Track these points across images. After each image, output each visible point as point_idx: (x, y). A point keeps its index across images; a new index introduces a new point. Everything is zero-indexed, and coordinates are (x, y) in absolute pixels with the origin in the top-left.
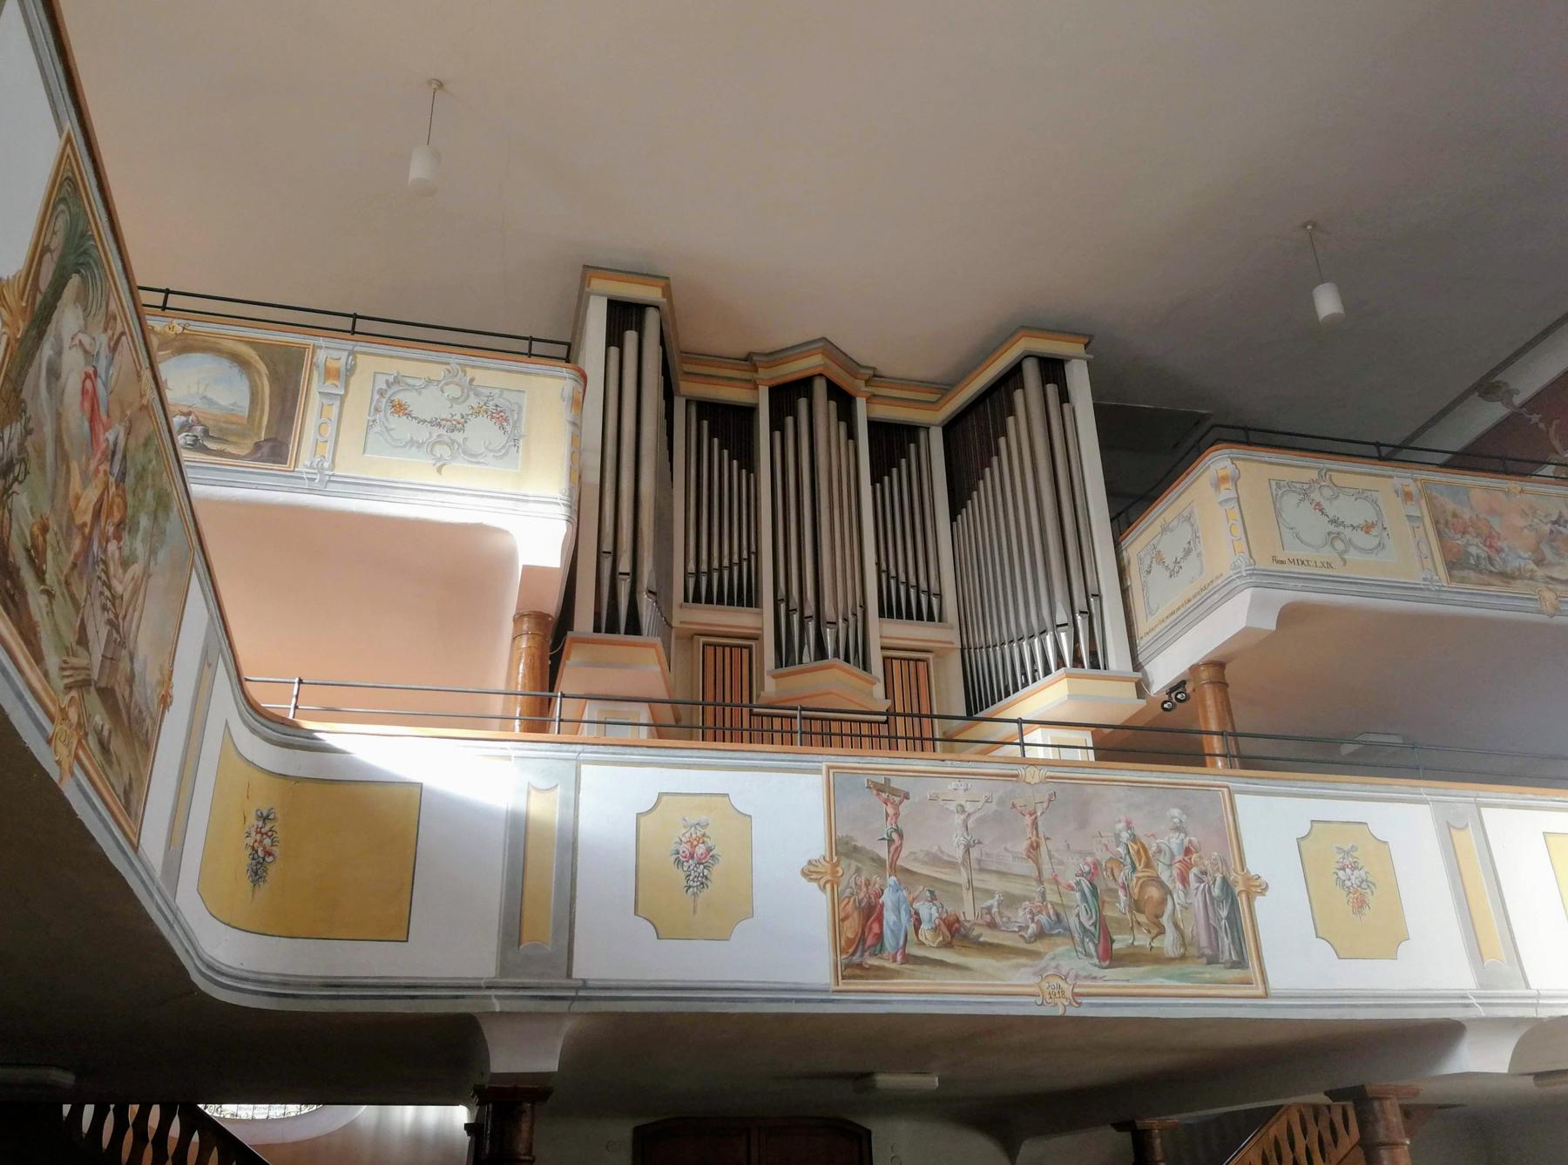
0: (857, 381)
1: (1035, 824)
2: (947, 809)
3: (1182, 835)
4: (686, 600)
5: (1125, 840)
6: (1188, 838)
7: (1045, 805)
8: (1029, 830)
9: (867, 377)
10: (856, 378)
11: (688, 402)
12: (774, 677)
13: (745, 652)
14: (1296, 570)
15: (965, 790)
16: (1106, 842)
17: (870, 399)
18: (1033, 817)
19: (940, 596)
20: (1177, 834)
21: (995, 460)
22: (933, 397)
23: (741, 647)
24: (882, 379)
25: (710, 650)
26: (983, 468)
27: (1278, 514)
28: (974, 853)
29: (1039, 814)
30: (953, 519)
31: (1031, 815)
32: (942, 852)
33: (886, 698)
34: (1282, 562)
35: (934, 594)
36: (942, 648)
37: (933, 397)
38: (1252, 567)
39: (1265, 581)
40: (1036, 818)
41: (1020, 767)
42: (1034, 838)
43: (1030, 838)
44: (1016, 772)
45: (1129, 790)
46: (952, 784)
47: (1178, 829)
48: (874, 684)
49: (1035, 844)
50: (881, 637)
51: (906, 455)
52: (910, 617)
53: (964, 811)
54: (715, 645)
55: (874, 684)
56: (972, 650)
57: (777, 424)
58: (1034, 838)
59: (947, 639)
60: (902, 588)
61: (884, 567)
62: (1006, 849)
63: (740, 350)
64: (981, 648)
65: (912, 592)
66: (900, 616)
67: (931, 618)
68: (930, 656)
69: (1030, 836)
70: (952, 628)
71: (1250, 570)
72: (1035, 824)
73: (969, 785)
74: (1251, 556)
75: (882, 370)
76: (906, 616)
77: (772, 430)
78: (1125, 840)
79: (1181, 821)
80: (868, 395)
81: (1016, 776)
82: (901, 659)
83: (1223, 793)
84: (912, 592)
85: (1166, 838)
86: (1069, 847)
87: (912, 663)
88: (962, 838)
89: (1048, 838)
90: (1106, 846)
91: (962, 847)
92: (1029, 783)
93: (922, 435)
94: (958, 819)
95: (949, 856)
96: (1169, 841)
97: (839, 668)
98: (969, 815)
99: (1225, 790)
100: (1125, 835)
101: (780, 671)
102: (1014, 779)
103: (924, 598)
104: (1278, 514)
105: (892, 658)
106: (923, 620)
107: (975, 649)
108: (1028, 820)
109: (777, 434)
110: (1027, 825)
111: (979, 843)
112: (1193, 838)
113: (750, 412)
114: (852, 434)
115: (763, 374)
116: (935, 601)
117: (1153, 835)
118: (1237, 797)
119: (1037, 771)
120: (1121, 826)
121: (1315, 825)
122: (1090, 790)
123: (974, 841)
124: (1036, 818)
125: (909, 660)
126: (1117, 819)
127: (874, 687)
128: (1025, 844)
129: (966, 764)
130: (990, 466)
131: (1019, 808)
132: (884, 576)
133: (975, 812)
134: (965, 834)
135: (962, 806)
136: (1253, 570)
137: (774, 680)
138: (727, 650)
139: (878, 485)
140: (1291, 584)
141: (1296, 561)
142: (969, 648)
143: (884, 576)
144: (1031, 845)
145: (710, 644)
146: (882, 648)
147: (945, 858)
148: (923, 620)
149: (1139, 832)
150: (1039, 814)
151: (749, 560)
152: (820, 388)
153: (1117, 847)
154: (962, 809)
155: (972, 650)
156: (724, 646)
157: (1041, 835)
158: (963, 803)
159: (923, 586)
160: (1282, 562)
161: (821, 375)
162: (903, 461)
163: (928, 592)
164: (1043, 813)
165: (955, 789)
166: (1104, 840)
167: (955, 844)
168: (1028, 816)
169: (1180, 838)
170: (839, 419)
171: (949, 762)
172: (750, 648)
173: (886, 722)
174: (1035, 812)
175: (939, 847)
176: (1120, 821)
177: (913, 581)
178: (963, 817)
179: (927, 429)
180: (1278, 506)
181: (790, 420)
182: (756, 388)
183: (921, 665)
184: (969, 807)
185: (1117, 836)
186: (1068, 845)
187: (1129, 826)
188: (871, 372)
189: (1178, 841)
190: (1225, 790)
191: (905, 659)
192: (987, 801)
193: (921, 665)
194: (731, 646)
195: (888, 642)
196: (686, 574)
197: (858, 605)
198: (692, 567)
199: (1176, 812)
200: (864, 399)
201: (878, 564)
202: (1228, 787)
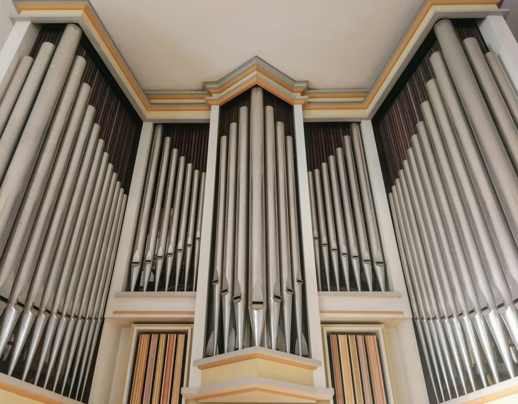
0: (294, 94)
4: (128, 288)
9: (302, 90)
10: (293, 92)
11: (155, 125)
12: (202, 367)
13: (181, 337)
17: (305, 107)
19: (384, 263)
21: (420, 126)
22: (361, 99)
23: (177, 333)
24: (316, 91)
25: (145, 338)
26: (410, 137)
30: (389, 190)
35: (378, 263)
36: (394, 319)
37: (361, 99)
48: (316, 368)
50: (321, 312)
51: (341, 145)
52: (354, 287)
54: (150, 333)
55: (313, 368)
56: (425, 320)
57: (223, 130)
61: (324, 240)
63: (195, 83)
64: (434, 318)
65: (355, 263)
66: (343, 287)
67: (376, 287)
75: (315, 83)
76: (350, 287)
77: (220, 135)
80: (303, 102)
82: (348, 334)
84: (355, 263)
87: (360, 338)
93: (355, 130)
97: (263, 357)
101: (208, 360)
103: (367, 267)
105: (337, 333)
106: (380, 290)
107: (428, 319)
109: (224, 138)
113: (205, 127)
114: (290, 131)
115: (215, 96)
125: (356, 334)
127: (314, 371)
130: (417, 132)
132: (325, 249)
137: (201, 371)
139: (317, 171)
142: (422, 319)
143: (325, 249)
145: (146, 333)
146: (323, 323)
148: (380, 290)
152: (257, 98)
155: (425, 320)
156: (159, 333)
159: (366, 255)
161: (256, 86)
162: (339, 150)
170: (276, 119)
172: (185, 333)
177: (354, 252)
179: (359, 123)
181: (233, 126)
182: (210, 109)
183: (371, 339)
188: (305, 85)
194: (167, 333)
195: (329, 317)
196: (131, 264)
197: (295, 280)
198: (137, 257)
200: (301, 106)
201: (319, 238)
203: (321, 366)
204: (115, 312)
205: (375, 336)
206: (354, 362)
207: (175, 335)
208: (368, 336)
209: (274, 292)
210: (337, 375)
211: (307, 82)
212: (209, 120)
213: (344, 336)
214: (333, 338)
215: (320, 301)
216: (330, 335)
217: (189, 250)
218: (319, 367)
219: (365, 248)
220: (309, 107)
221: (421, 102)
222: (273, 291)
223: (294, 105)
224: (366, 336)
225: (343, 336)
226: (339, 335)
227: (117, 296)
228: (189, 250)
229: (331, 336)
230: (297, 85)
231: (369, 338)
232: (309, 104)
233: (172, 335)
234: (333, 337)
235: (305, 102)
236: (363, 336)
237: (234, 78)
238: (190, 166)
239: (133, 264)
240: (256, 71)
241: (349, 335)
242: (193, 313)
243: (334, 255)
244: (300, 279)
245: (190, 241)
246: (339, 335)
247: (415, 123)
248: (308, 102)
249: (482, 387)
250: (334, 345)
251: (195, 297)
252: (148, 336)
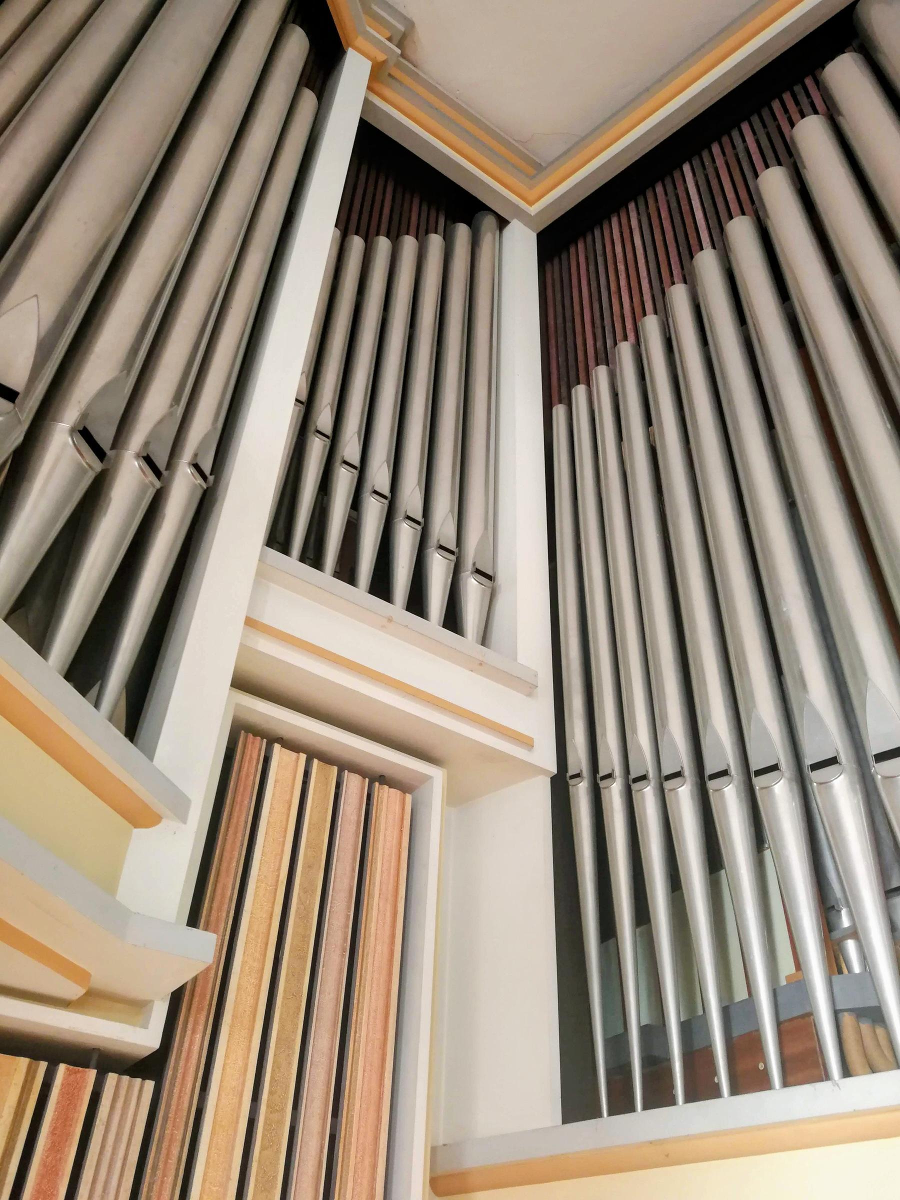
33: (193, 921)
61: (324, 419)
70: (529, 688)
80: (381, 57)
93: (488, 223)
105: (272, 739)
116: (472, 588)
125: (344, 766)
132: (316, 448)
143: (316, 448)
163: (456, 554)
179: (502, 223)
188: (401, 28)
191: (327, 759)
200: (368, 65)
203: (184, 820)
206: (308, 866)
208: (386, 787)
209: (90, 406)
210: (218, 897)
211: (410, 25)
213: (298, 758)
214: (253, 749)
216: (243, 732)
219: (450, 511)
221: (758, 171)
222: (83, 405)
223: (349, 45)
224: (377, 784)
225: (294, 755)
226: (277, 747)
229: (246, 738)
231: (386, 795)
232: (390, 80)
234: (253, 743)
235: (385, 62)
236: (367, 780)
241: (316, 761)
243: (343, 481)
244: (207, 467)
246: (277, 747)
247: (688, 252)
248: (390, 75)
249: (630, 1108)
250: (247, 776)
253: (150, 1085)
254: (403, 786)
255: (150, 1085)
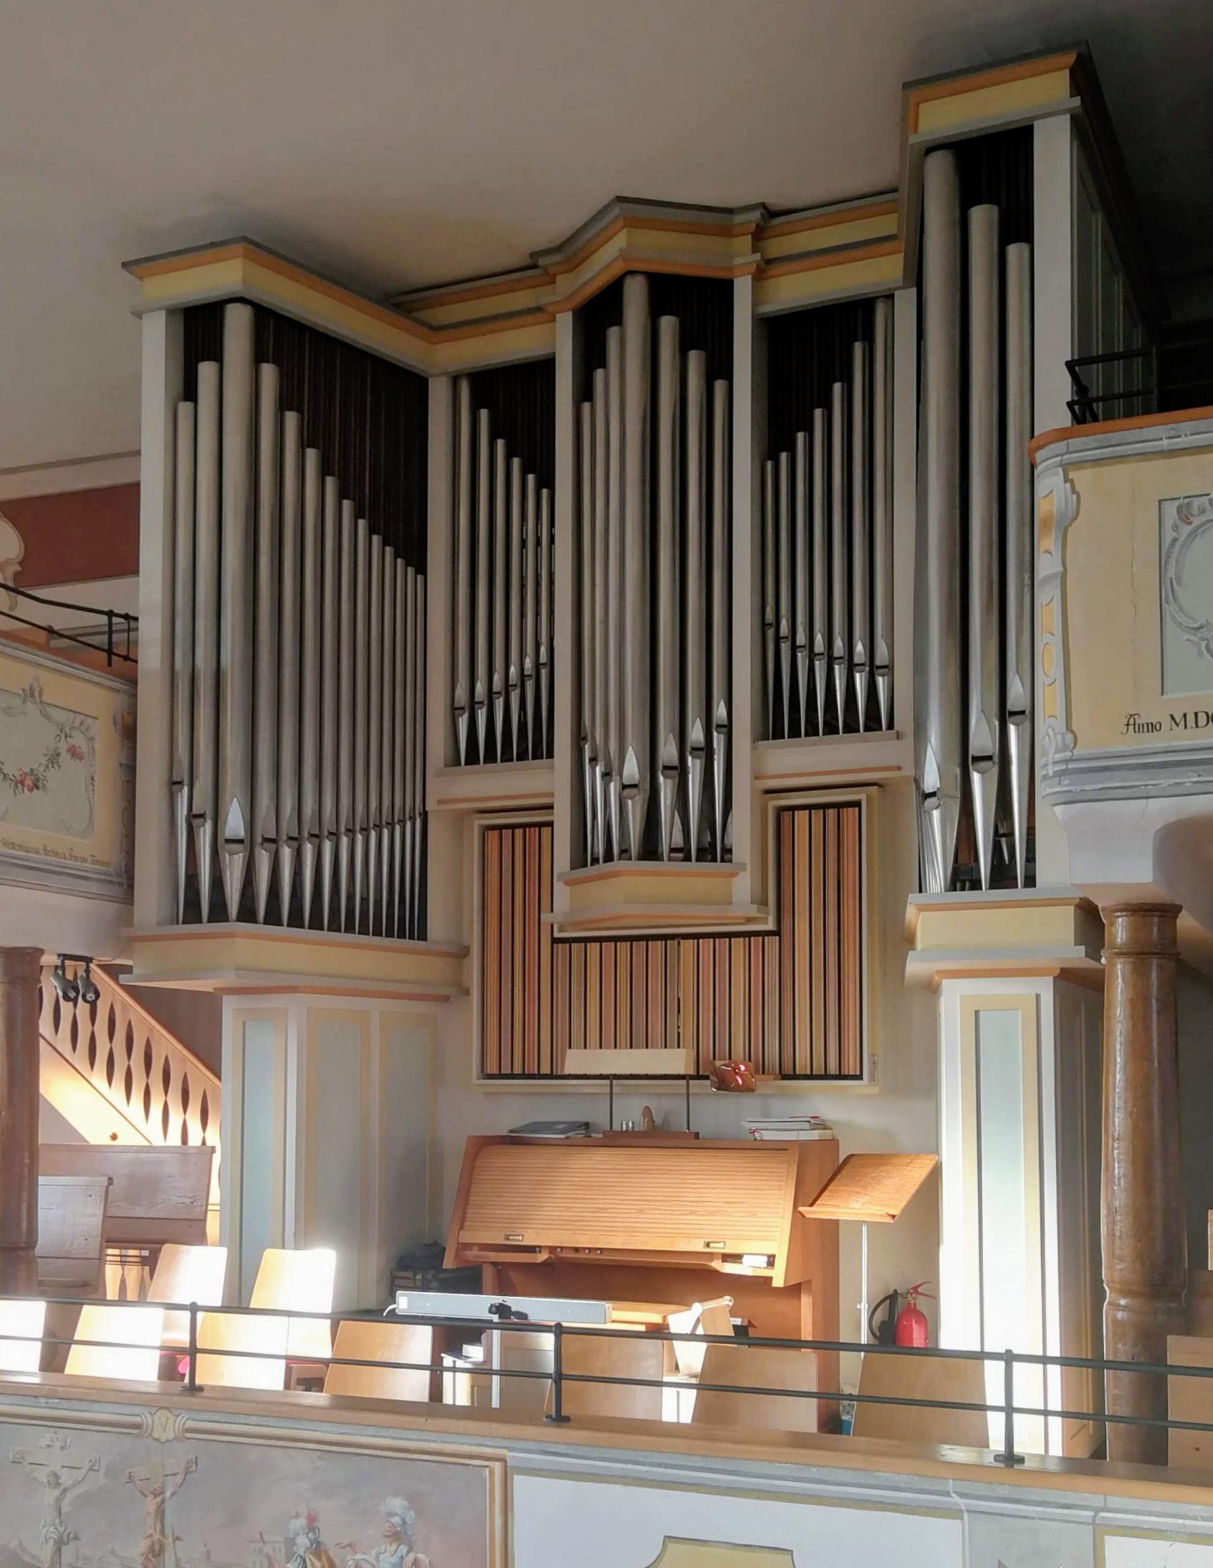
1: (160, 1513)
2: (35, 1479)
3: (403, 1549)
5: (301, 1551)
6: (412, 1556)
7: (179, 1479)
8: (151, 1520)
14: (1187, 743)
15: (63, 1448)
16: (271, 1553)
18: (159, 1499)
19: (889, 668)
20: (394, 1546)
27: (1167, 590)
28: (68, 1553)
29: (168, 1494)
31: (156, 1496)
32: (24, 1550)
34: (1152, 727)
38: (1069, 754)
39: (1092, 785)
40: (163, 1502)
41: (145, 1411)
42: (157, 1536)
43: (151, 1535)
44: (137, 1420)
45: (320, 1458)
46: (46, 1436)
47: (397, 1536)
49: (157, 1547)
53: (58, 1484)
54: (500, 828)
55: (734, 875)
57: (584, 392)
58: (157, 1536)
59: (893, 763)
60: (820, 667)
62: (113, 1552)
68: (859, 795)
69: (152, 1531)
71: (1062, 761)
72: (160, 1513)
73: (69, 1440)
74: (1069, 727)
78: (301, 1551)
79: (404, 1522)
81: (137, 1426)
83: (492, 1473)
85: (374, 1553)
86: (209, 1558)
88: (52, 1529)
89: (178, 1538)
90: (269, 1558)
91: (52, 1542)
92: (157, 1440)
94: (51, 1495)
95: (33, 1556)
96: (377, 1556)
98: (65, 1490)
99: (497, 1466)
100: (303, 1541)
101: (581, 872)
102: (136, 1431)
104: (1167, 590)
105: (793, 808)
108: (151, 1504)
110: (149, 1514)
111: (76, 1538)
112: (421, 1556)
117: (350, 1545)
118: (518, 1480)
119: (172, 1418)
120: (301, 1522)
121: (671, 1546)
122: (254, 1454)
123: (69, 1534)
124: (163, 1502)
125: (824, 807)
126: (293, 1513)
128: (143, 1545)
129: (65, 1404)
131: (139, 1483)
133: (74, 1486)
134: (57, 1521)
135: (56, 1476)
136: (1071, 760)
137: (568, 888)
138: (519, 832)
140: (1165, 780)
141: (1191, 719)
144: (151, 1549)
147: (27, 1559)
149: (329, 1539)
150: (168, 1494)
151: (537, 666)
153: (288, 1563)
154: (55, 1480)
157: (168, 1532)
158: (58, 1470)
160: (1152, 727)
164: (173, 1494)
165: (49, 1446)
166: (268, 1549)
167: (42, 1538)
168: (151, 1496)
169: (399, 1554)
171: (43, 1400)
173: (777, 933)
174: (163, 1492)
175: (20, 1542)
176: (297, 1516)
178: (56, 1493)
180: (1171, 573)
184: (66, 1478)
185: (290, 1542)
186: (208, 1552)
187: (312, 1523)
189: (394, 1560)
190: (497, 1466)
192: (91, 1469)
193: (850, 814)
194: (524, 826)
196: (454, 711)
199: (397, 1504)
202: (503, 1460)
204: (440, 802)
205: (857, 809)
207: (537, 829)
212: (555, 353)
214: (787, 816)
215: (756, 760)
217: (544, 672)
218: (742, 874)
220: (772, 272)
227: (439, 775)
228: (544, 672)
230: (738, 219)
233: (532, 829)
237: (590, 241)
238: (531, 478)
239: (457, 712)
240: (625, 230)
242: (552, 795)
245: (543, 658)
251: (552, 767)
252: (496, 832)
253: (777, 937)
254: (857, 804)
255: (777, 937)
